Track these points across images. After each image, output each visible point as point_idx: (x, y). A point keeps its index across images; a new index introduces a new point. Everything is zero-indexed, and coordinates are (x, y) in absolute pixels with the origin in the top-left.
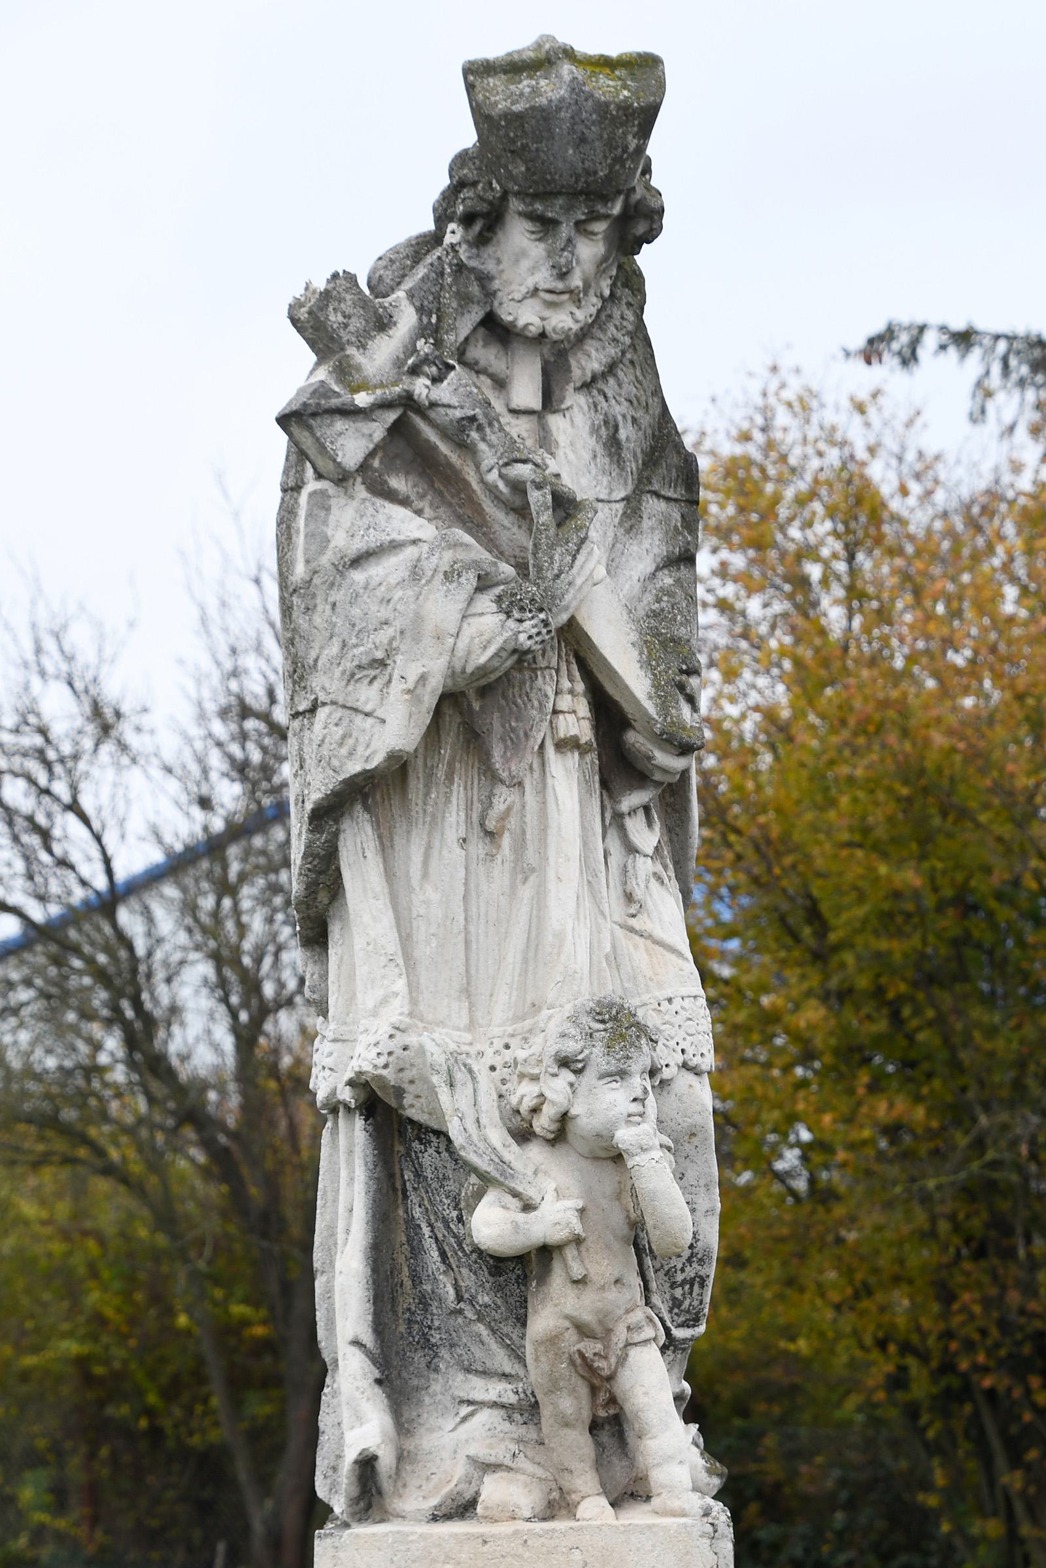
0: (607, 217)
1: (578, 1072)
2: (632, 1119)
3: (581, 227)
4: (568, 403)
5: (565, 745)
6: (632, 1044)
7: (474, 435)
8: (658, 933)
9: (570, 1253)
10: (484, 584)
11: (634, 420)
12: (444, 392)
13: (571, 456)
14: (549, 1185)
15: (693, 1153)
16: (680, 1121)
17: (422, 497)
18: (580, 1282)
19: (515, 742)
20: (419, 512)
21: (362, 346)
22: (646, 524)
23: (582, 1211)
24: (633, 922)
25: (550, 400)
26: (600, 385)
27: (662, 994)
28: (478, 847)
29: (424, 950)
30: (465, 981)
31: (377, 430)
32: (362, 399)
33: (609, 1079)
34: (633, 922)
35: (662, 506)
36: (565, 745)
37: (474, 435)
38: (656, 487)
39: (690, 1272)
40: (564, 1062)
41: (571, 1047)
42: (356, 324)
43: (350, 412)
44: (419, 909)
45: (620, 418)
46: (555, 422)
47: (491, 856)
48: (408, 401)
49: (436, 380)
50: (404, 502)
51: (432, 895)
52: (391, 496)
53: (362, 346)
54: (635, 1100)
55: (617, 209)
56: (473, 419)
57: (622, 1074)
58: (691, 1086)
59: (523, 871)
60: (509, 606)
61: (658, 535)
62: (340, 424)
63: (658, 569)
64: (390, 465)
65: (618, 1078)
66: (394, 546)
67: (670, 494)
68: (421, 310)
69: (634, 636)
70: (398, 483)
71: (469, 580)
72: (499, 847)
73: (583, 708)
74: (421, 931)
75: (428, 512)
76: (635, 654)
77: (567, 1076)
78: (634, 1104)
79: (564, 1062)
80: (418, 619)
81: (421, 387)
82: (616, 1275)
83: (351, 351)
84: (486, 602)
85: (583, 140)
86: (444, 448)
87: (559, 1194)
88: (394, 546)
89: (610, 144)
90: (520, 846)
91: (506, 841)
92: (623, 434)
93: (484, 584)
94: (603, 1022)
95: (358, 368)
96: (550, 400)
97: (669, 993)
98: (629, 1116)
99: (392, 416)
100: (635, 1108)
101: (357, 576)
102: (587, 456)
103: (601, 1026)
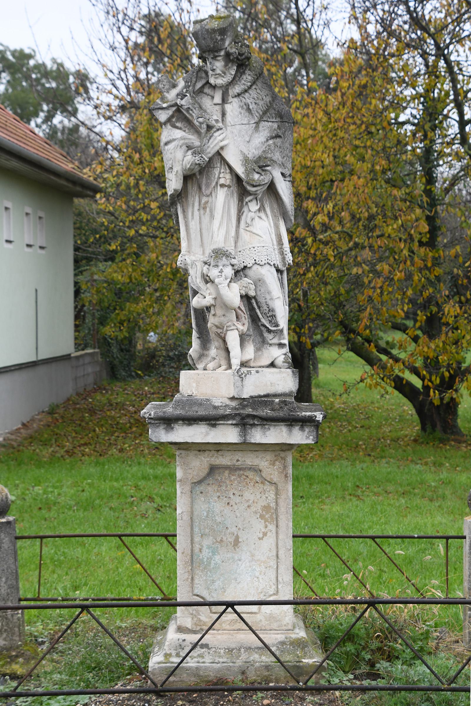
0: (220, 56)
1: (209, 265)
3: (215, 58)
4: (230, 101)
5: (222, 186)
7: (191, 112)
8: (254, 231)
9: (212, 308)
10: (189, 148)
11: (255, 103)
12: (183, 102)
13: (231, 114)
14: (208, 292)
17: (186, 127)
18: (214, 315)
19: (208, 185)
20: (185, 131)
21: (168, 92)
22: (261, 128)
23: (215, 299)
24: (247, 229)
25: (224, 101)
26: (243, 95)
27: (250, 246)
28: (202, 211)
29: (193, 236)
31: (170, 112)
32: (165, 105)
34: (247, 229)
35: (270, 123)
36: (222, 186)
37: (191, 112)
38: (265, 119)
39: (271, 314)
40: (206, 263)
41: (205, 259)
42: (167, 87)
43: (163, 109)
44: (191, 226)
45: (250, 104)
46: (228, 107)
47: (204, 214)
48: (176, 104)
49: (182, 99)
50: (180, 129)
51: (193, 223)
52: (177, 128)
53: (168, 92)
55: (222, 53)
56: (189, 108)
57: (217, 266)
59: (212, 217)
60: (194, 153)
61: (266, 132)
62: (160, 111)
63: (267, 140)
64: (177, 121)
66: (174, 140)
67: (274, 120)
68: (186, 82)
69: (242, 158)
70: (178, 124)
71: (184, 148)
72: (206, 211)
73: (228, 176)
74: (192, 231)
75: (187, 131)
76: (241, 162)
77: (207, 266)
79: (206, 263)
80: (175, 157)
81: (179, 101)
82: (223, 313)
83: (165, 94)
84: (190, 152)
85: (204, 39)
86: (187, 115)
87: (210, 294)
88: (174, 140)
89: (212, 39)
90: (211, 211)
91: (208, 209)
92: (251, 107)
93: (189, 148)
95: (167, 98)
96: (224, 101)
99: (174, 109)
100: (220, 274)
101: (166, 147)
102: (237, 113)
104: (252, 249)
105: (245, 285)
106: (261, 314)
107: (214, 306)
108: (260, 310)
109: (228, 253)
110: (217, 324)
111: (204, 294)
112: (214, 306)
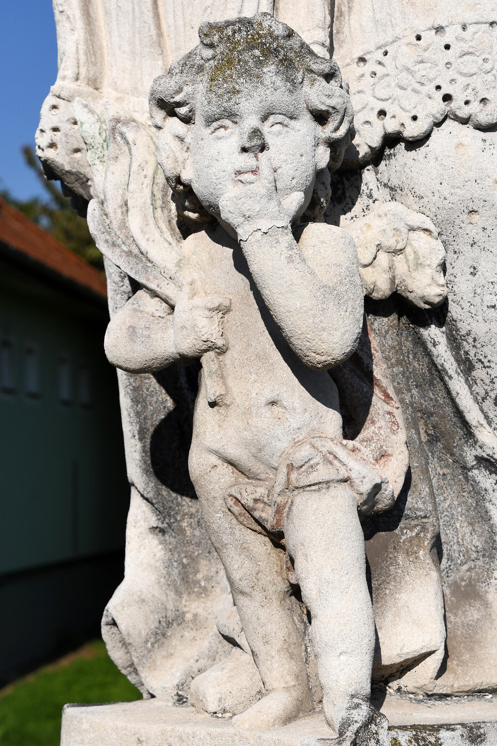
1: (187, 120)
2: (243, 177)
6: (247, 72)
15: (481, 237)
16: (446, 194)
30: (154, 32)
33: (215, 125)
54: (244, 150)
58: (460, 145)
65: (227, 122)
78: (246, 154)
94: (211, 46)
97: (440, 22)
98: (239, 173)
100: (247, 160)
103: (208, 53)
104: (429, 36)
105: (390, 242)
106: (479, 401)
107: (222, 351)
108: (470, 383)
109: (294, 43)
110: (233, 452)
111: (167, 290)
112: (222, 351)
